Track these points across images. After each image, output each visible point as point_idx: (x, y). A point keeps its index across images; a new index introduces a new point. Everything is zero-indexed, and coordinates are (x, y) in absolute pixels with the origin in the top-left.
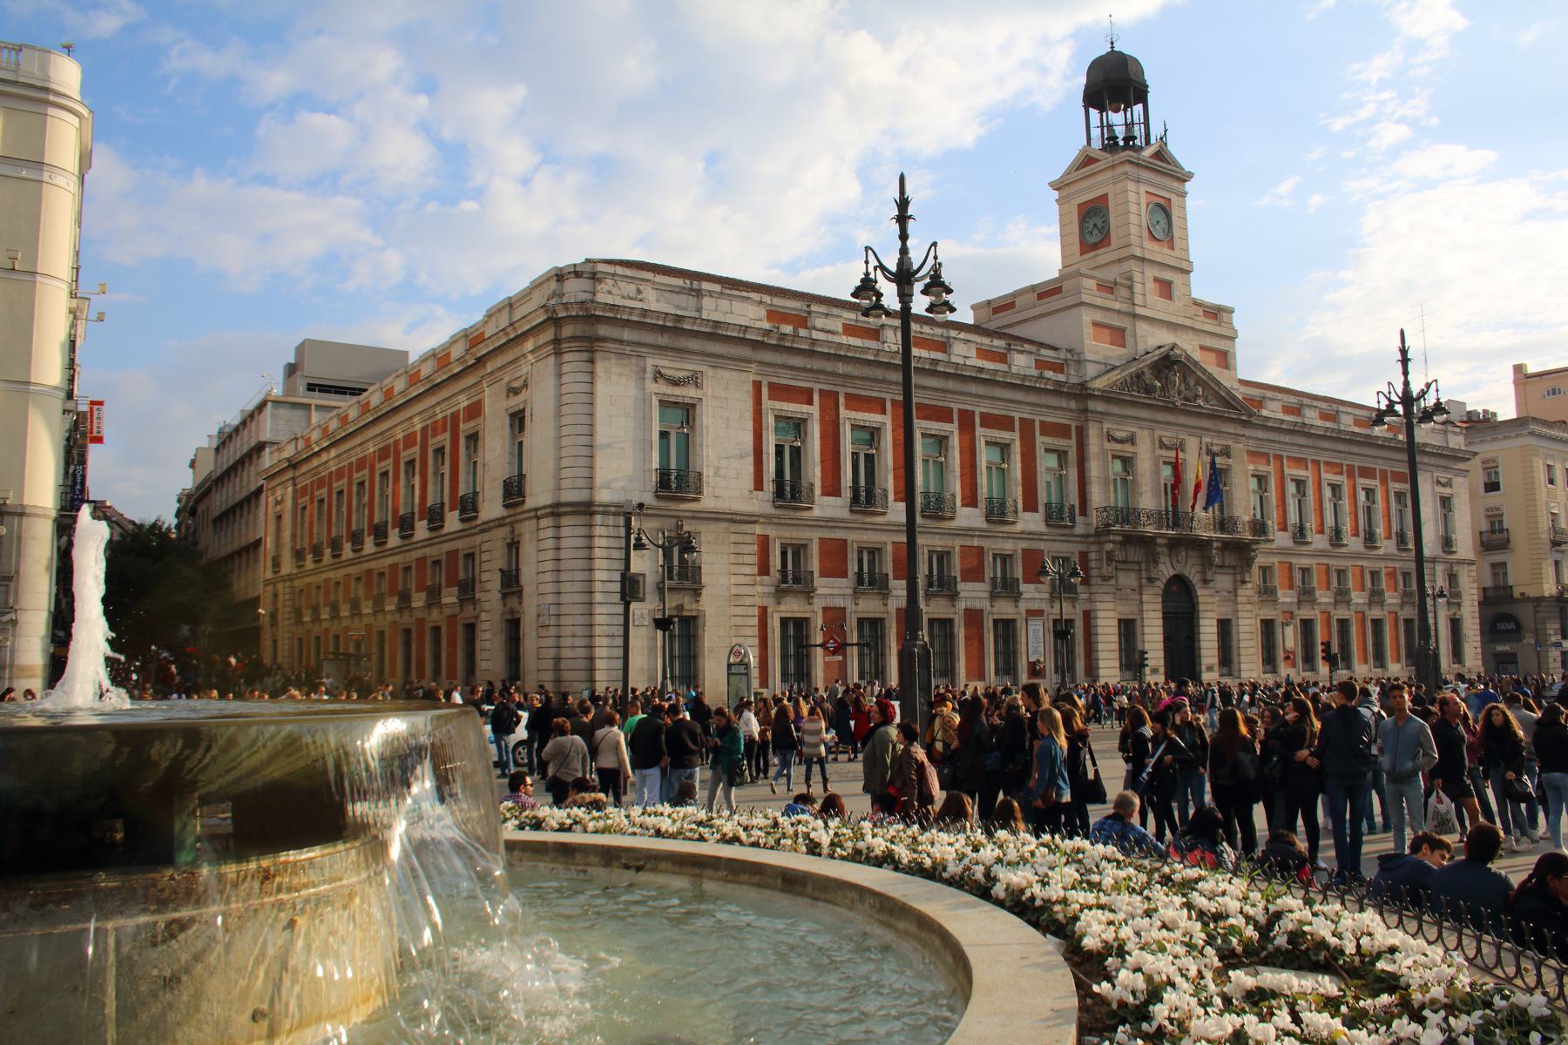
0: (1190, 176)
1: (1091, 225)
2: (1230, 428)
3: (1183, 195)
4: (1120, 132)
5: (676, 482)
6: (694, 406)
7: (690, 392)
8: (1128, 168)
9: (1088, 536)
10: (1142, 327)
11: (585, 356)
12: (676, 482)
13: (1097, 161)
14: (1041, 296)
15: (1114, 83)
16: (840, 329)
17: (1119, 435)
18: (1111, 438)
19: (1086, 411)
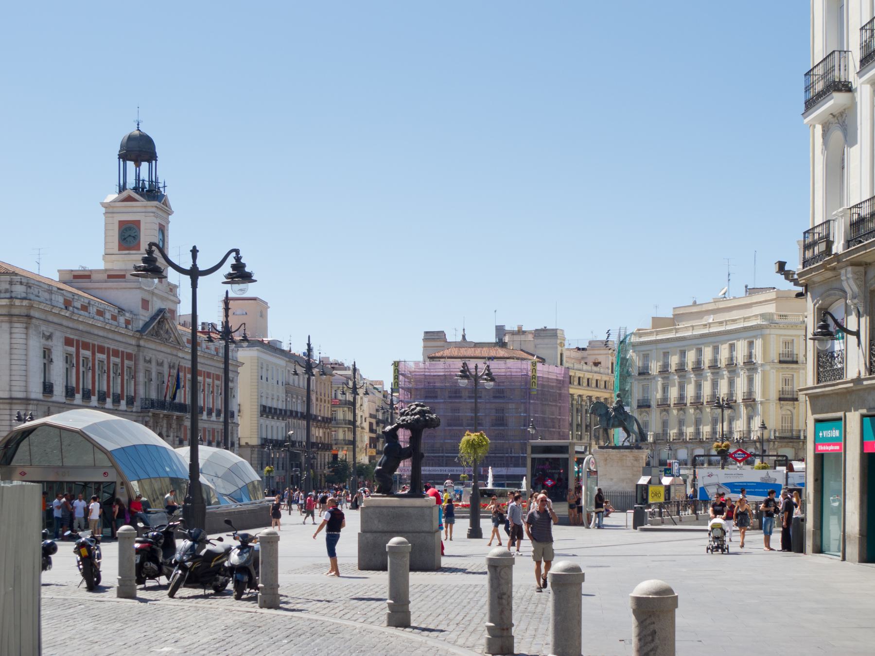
0: (173, 212)
1: (128, 235)
2: (175, 352)
3: (168, 222)
4: (147, 184)
5: (48, 388)
6: (49, 350)
7: (49, 343)
8: (154, 209)
9: (137, 412)
10: (155, 299)
11: (25, 325)
12: (48, 388)
13: (134, 200)
14: (109, 277)
15: (139, 149)
16: (79, 307)
17: (148, 358)
18: (145, 361)
19: (139, 346)
